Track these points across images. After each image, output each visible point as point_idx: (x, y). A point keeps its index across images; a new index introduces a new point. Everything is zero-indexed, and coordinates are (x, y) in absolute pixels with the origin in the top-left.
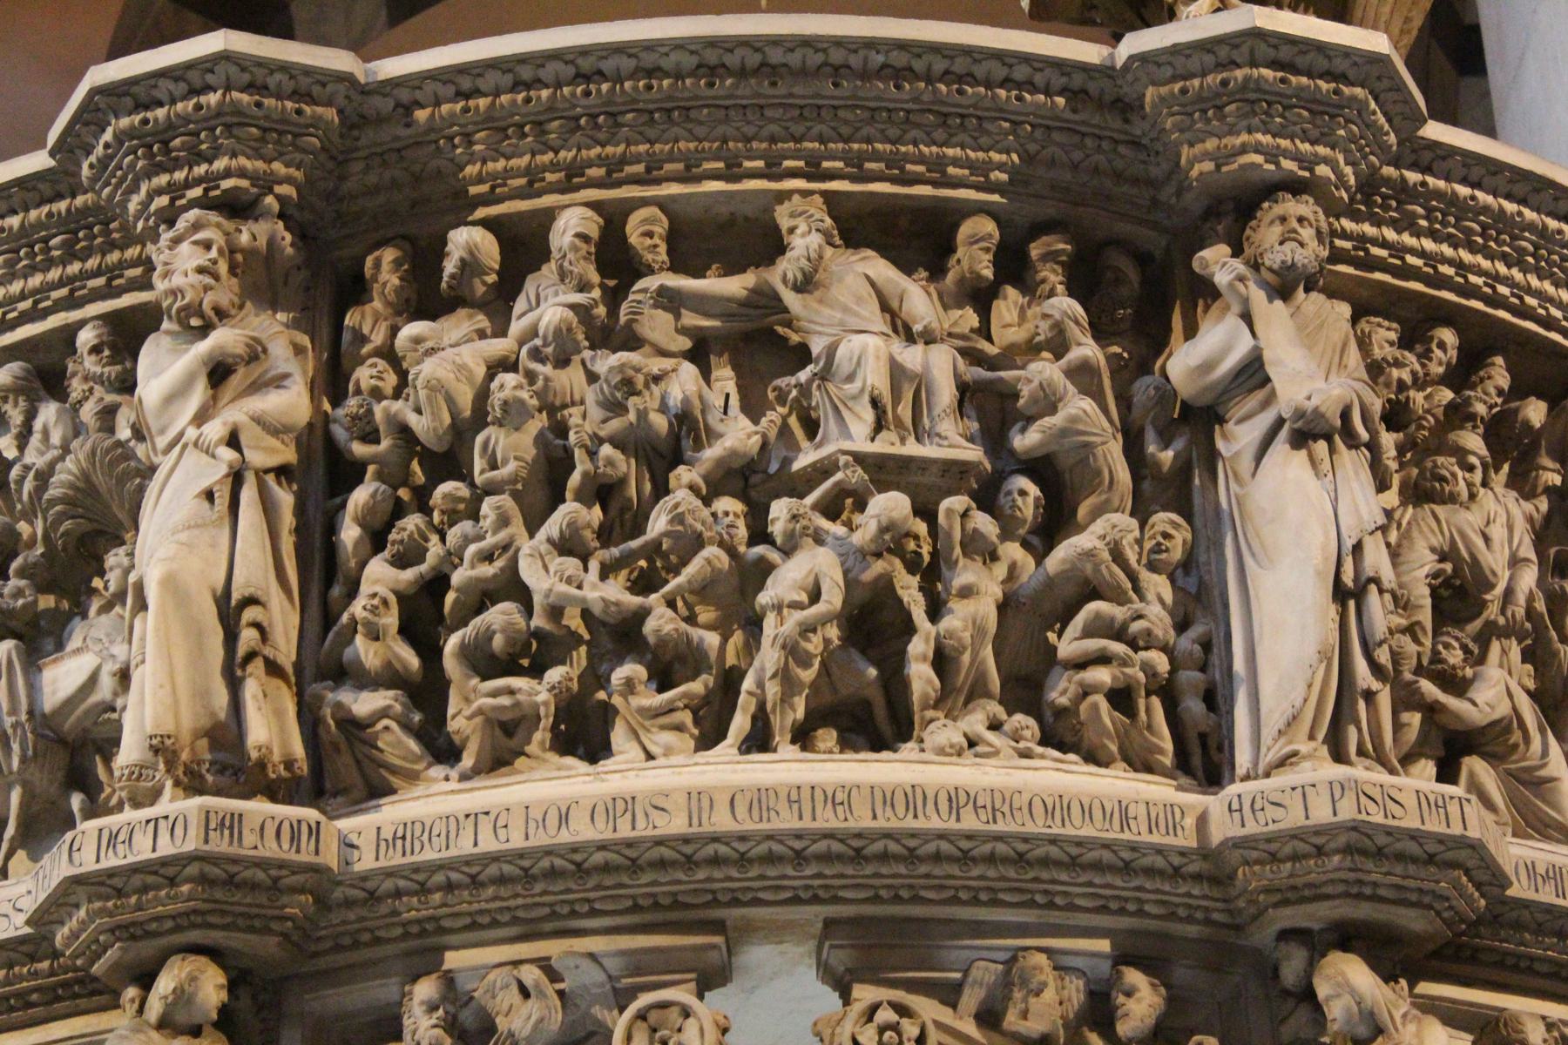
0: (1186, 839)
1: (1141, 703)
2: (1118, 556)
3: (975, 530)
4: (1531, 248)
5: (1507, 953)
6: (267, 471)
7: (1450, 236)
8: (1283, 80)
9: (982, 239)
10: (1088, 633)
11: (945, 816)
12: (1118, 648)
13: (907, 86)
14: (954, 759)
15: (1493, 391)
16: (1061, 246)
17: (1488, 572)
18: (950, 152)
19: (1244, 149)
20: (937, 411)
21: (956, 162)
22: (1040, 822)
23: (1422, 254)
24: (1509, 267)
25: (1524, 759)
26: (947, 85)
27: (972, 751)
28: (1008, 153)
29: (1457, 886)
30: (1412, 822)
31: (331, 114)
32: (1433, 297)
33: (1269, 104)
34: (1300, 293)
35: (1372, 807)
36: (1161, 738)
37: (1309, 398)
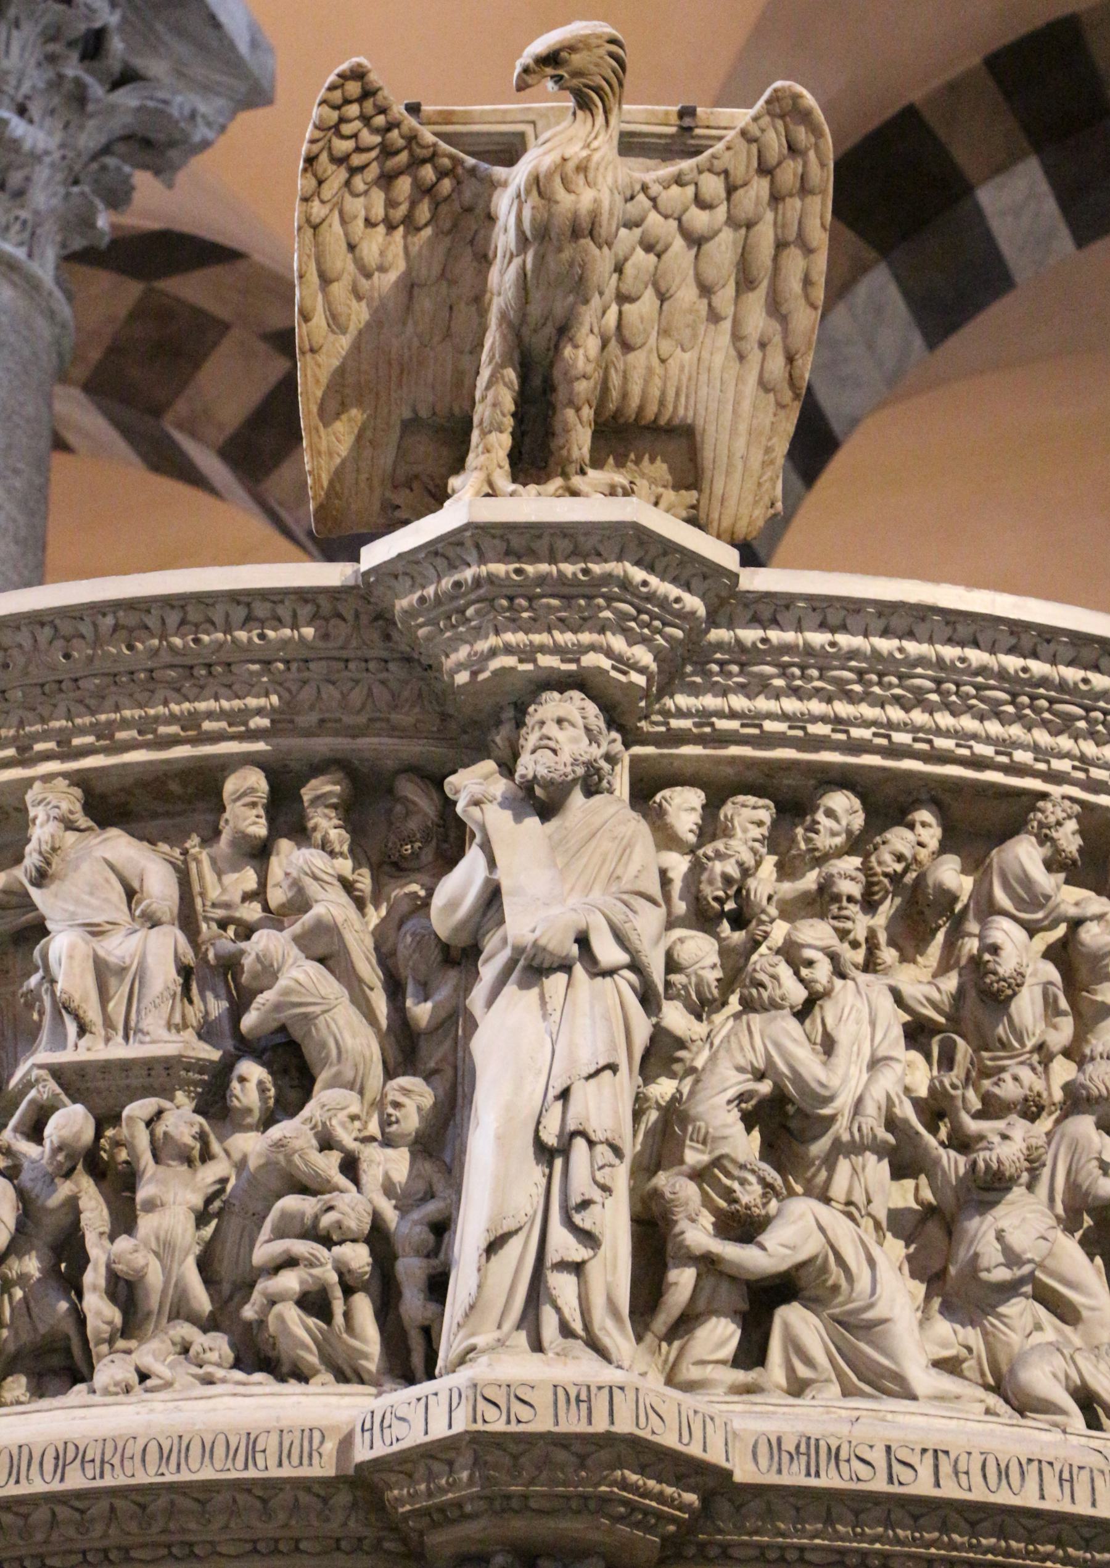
0: (324, 1467)
1: (338, 1307)
2: (327, 1143)
3: (165, 1134)
4: (929, 684)
5: (762, 1548)
7: (818, 690)
8: (518, 572)
9: (244, 794)
10: (280, 1233)
11: (48, 1478)
12: (302, 1247)
13: (139, 646)
14: (121, 1398)
15: (888, 858)
16: (328, 788)
17: (814, 1085)
18: (202, 706)
19: (493, 653)
20: (146, 1002)
21: (210, 715)
22: (152, 1470)
23: (784, 717)
24: (907, 710)
25: (850, 1300)
26: (183, 636)
27: (143, 1386)
28: (267, 695)
29: (624, 1485)
30: (542, 1424)
32: (809, 763)
33: (511, 599)
34: (577, 797)
35: (491, 1413)
36: (364, 1341)
37: (533, 931)
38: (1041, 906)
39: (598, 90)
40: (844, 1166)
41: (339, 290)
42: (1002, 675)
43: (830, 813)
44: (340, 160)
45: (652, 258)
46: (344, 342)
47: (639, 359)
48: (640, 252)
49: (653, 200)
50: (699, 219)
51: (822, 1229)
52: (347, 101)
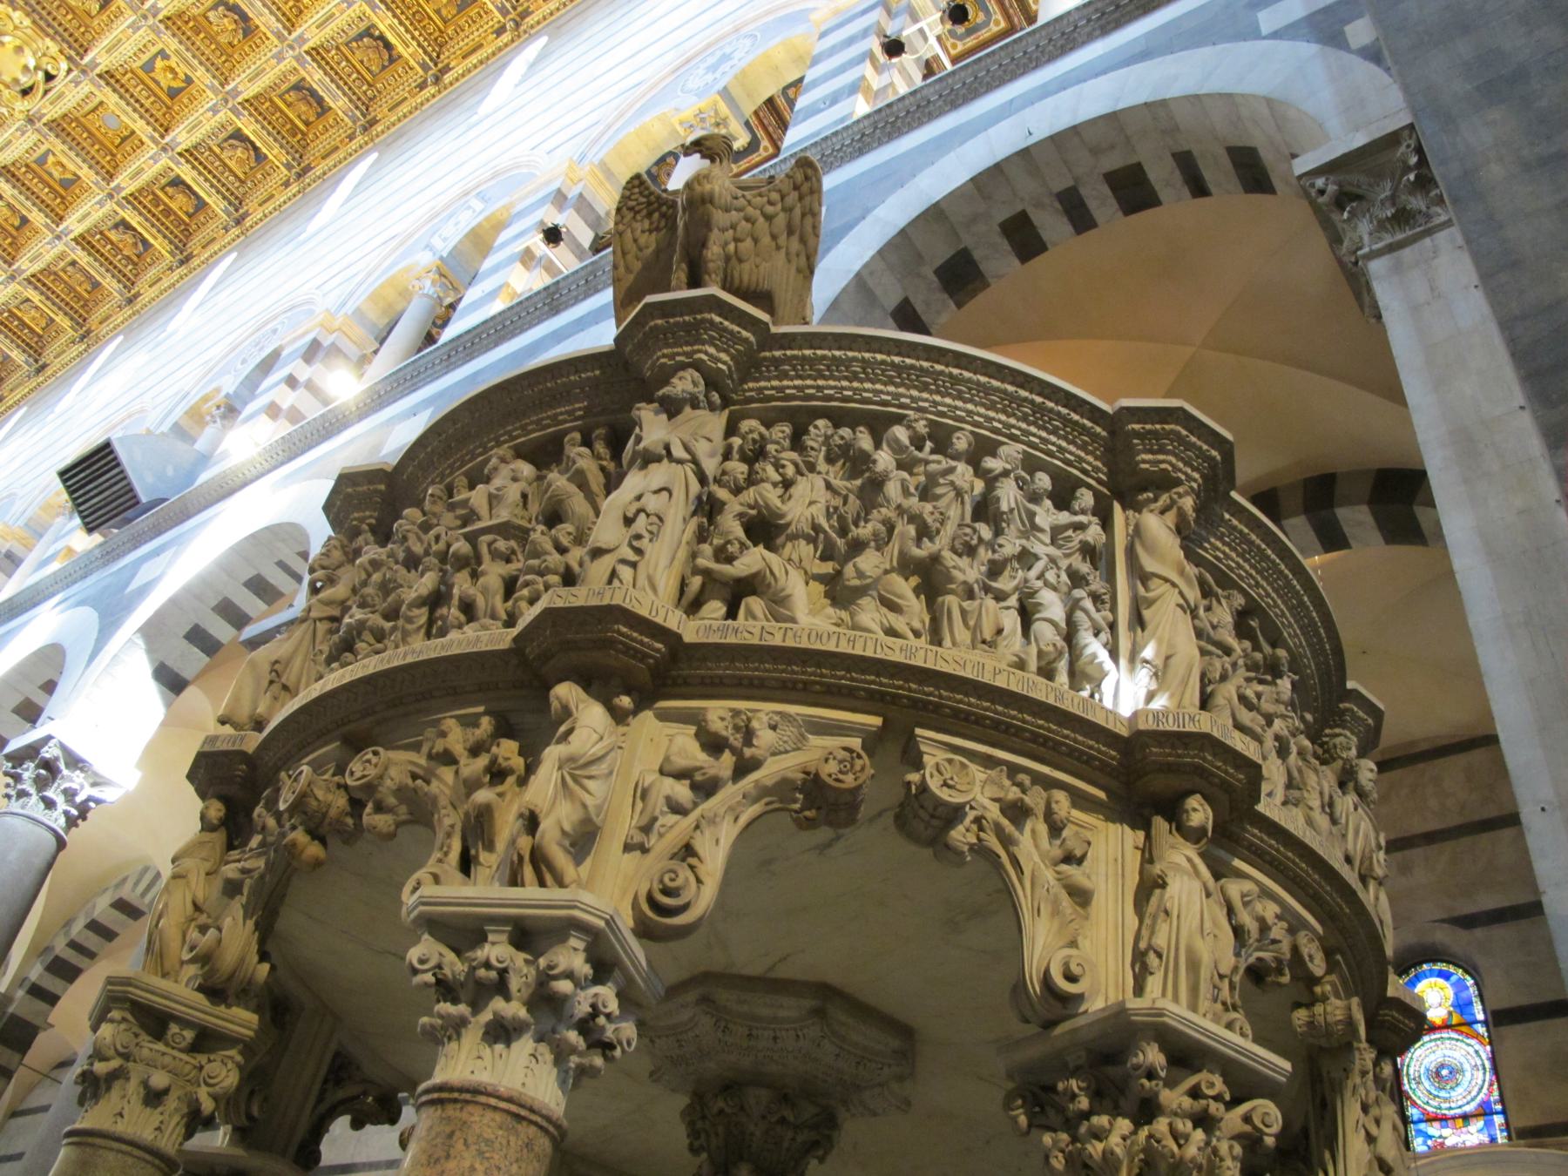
5: (703, 677)
6: (321, 620)
21: (562, 414)
23: (795, 387)
29: (619, 632)
31: (382, 487)
34: (688, 409)
38: (904, 452)
39: (719, 155)
40: (789, 545)
41: (629, 257)
42: (893, 364)
43: (816, 427)
44: (631, 209)
45: (749, 225)
46: (631, 277)
47: (746, 266)
48: (744, 223)
49: (749, 202)
50: (769, 209)
51: (764, 559)
52: (634, 187)
